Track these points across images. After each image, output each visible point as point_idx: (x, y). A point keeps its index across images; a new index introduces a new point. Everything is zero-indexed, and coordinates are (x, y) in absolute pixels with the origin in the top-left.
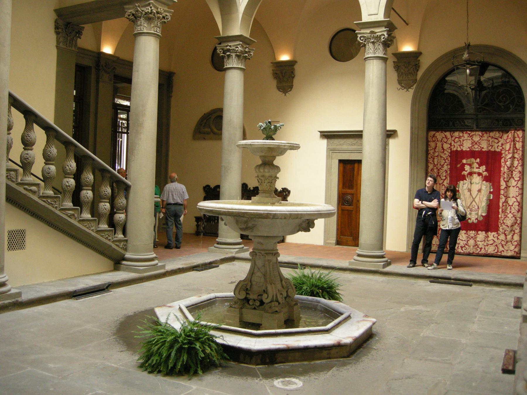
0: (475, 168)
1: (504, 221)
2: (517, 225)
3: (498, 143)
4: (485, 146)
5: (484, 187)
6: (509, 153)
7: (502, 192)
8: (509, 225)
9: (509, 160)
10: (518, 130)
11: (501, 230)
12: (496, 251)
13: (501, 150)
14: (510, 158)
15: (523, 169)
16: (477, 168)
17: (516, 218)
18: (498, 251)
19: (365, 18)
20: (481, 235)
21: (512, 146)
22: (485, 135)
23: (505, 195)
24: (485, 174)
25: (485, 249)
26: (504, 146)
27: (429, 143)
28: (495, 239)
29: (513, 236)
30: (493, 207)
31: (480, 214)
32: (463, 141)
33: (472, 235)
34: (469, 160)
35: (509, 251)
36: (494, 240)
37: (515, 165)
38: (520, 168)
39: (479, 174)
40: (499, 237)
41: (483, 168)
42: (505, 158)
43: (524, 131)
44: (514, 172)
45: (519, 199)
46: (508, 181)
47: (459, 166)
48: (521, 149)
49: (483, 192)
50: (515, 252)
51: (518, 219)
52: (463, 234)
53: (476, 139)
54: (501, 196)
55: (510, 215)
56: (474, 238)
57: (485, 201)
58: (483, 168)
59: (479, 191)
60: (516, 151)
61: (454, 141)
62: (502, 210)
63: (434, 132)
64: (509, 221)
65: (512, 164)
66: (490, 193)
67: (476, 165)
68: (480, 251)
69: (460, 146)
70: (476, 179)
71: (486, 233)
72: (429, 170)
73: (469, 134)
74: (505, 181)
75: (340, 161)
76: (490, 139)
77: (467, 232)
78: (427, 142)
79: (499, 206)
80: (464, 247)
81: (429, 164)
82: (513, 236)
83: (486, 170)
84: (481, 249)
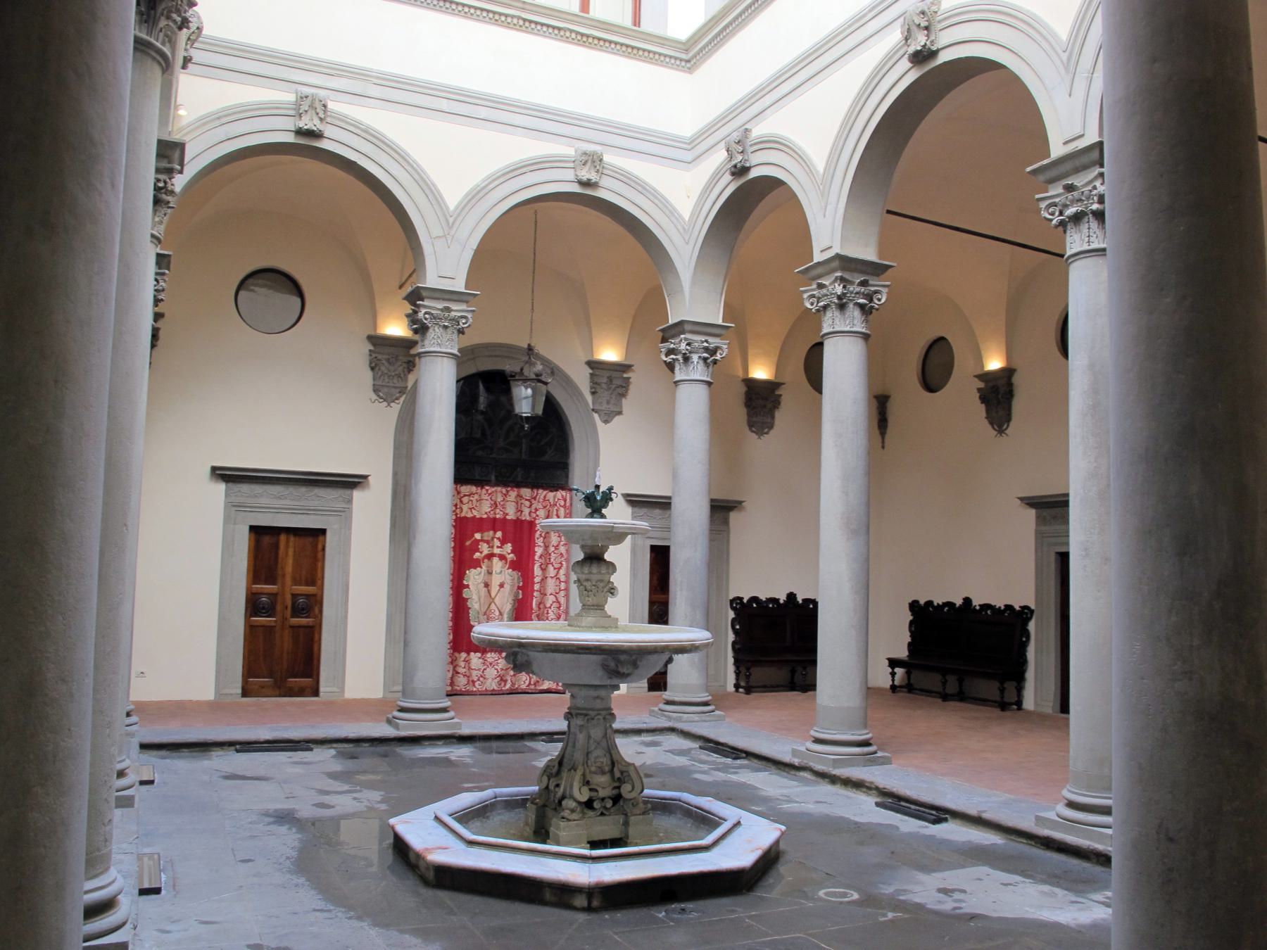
7: (537, 587)
39: (502, 557)
41: (509, 547)
47: (468, 543)
58: (509, 547)
59: (502, 586)
66: (519, 588)
67: (497, 543)
70: (497, 564)
75: (254, 529)
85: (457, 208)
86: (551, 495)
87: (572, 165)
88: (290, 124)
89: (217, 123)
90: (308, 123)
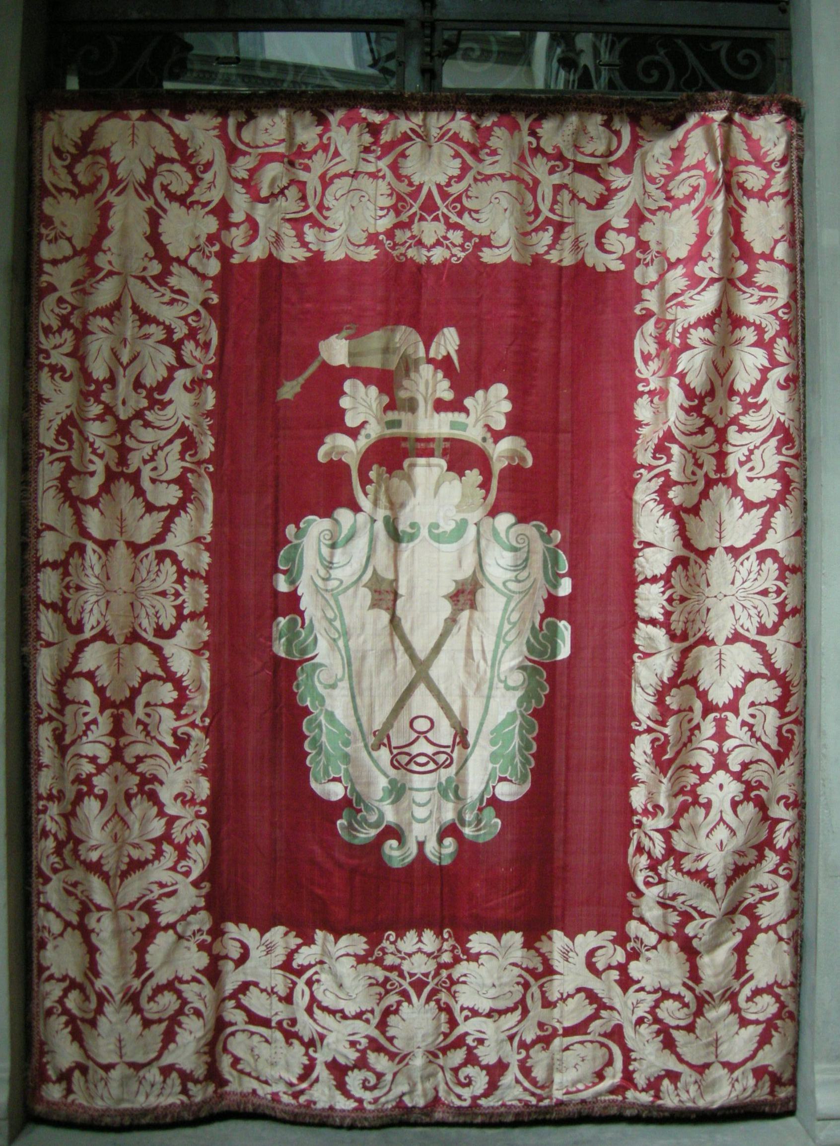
0: (424, 408)
1: (680, 842)
2: (771, 859)
3: (602, 203)
4: (498, 226)
5: (499, 565)
6: (695, 281)
7: (651, 600)
8: (716, 863)
9: (697, 336)
10: (756, 111)
11: (649, 909)
12: (614, 1077)
13: (630, 261)
14: (707, 322)
15: (801, 410)
16: (440, 406)
17: (762, 806)
18: (628, 1077)
20: (491, 965)
21: (716, 224)
22: (500, 138)
23: (677, 627)
24: (504, 451)
25: (526, 1070)
26: (649, 232)
27: (48, 206)
28: (607, 987)
29: (741, 950)
30: (573, 717)
31: (474, 787)
32: (326, 182)
33: (420, 966)
34: (375, 339)
35: (718, 1072)
36: (591, 996)
37: (743, 384)
38: (777, 403)
39: (461, 456)
40: (635, 969)
41: (494, 403)
42: (664, 324)
43: (794, 112)
44: (733, 434)
45: (779, 647)
46: (695, 510)
47: (289, 390)
48: (781, 252)
49: (493, 604)
50: (759, 1073)
51: (778, 811)
52: (345, 967)
53: (432, 168)
54: (644, 631)
55: (721, 790)
56: (438, 988)
57: (518, 678)
58: (494, 403)
59: (465, 595)
60: (742, 268)
61: (249, 184)
62: (658, 750)
63: (86, 118)
64: (714, 843)
65: (721, 367)
67: (430, 384)
68: (492, 1087)
69: (297, 223)
70: (437, 496)
71: (528, 944)
72: (47, 437)
73: (375, 130)
74: (678, 513)
76: (539, 167)
77: (374, 942)
78: (30, 193)
79: (630, 714)
80: (362, 1063)
81: (46, 384)
82: (741, 950)
83: (517, 424)
84: (497, 1070)
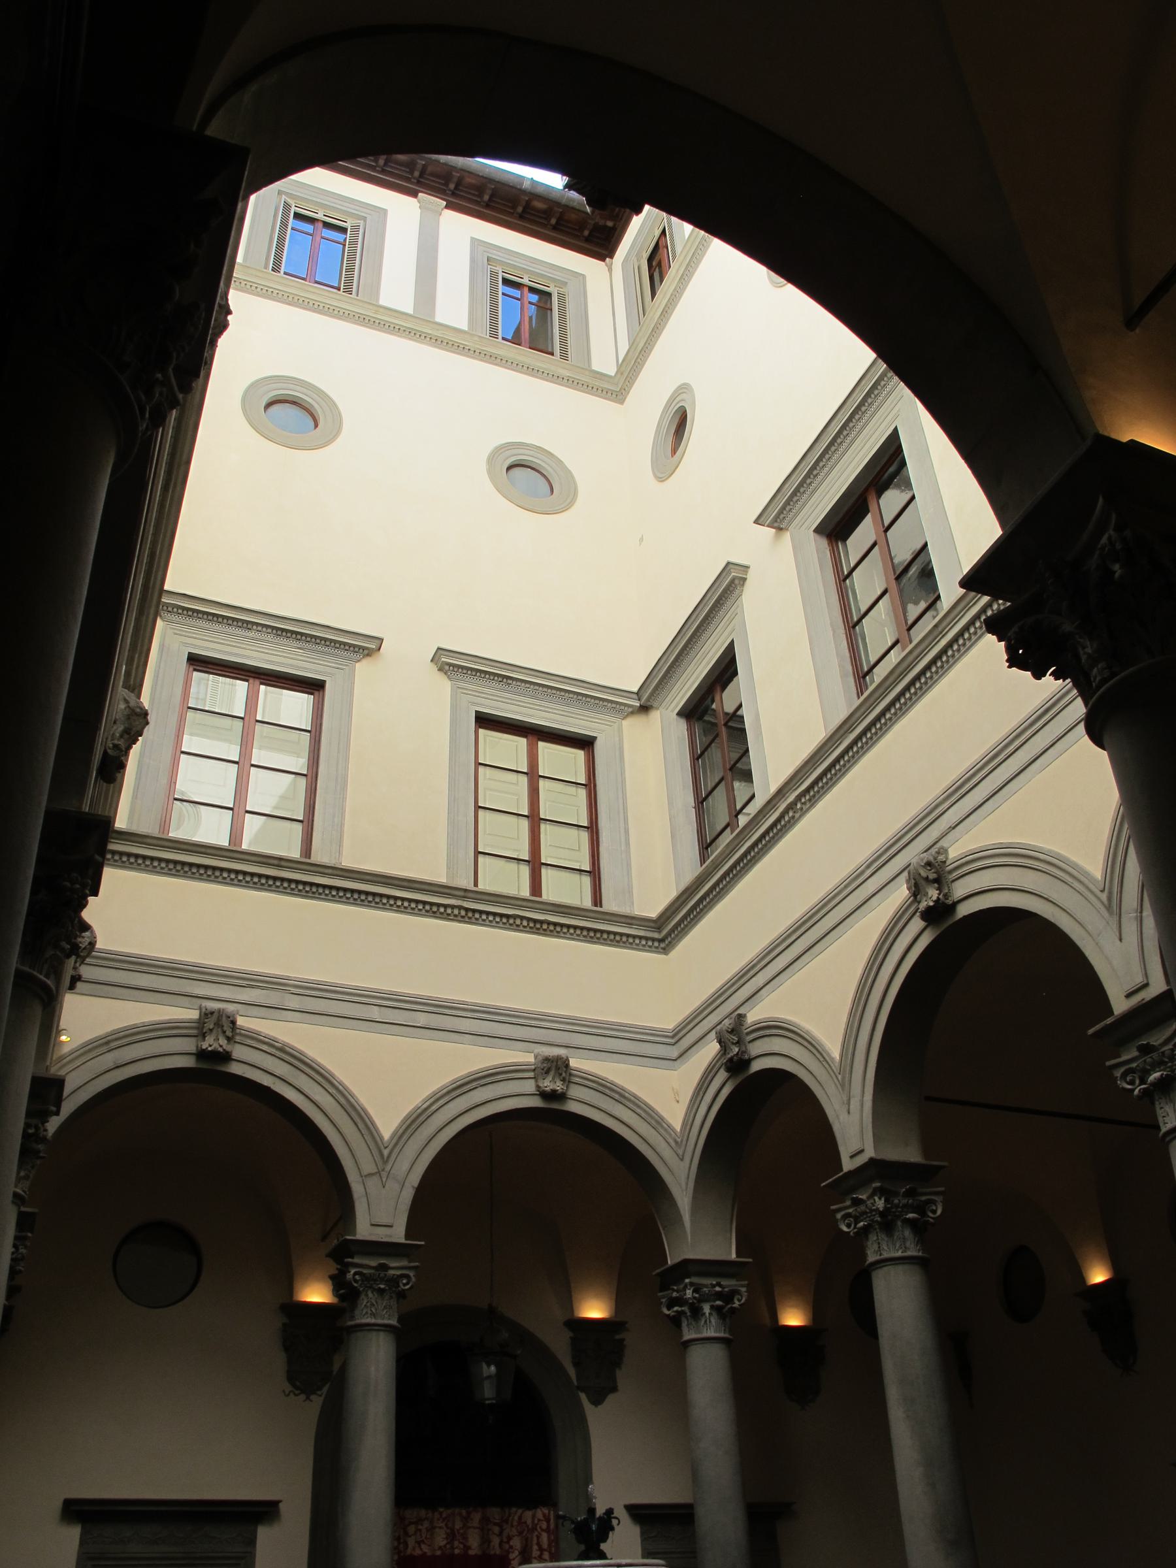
19: (364, 1230)
85: (392, 1137)
86: (528, 1515)
87: (531, 1074)
88: (189, 1045)
89: (105, 1049)
90: (210, 1043)
